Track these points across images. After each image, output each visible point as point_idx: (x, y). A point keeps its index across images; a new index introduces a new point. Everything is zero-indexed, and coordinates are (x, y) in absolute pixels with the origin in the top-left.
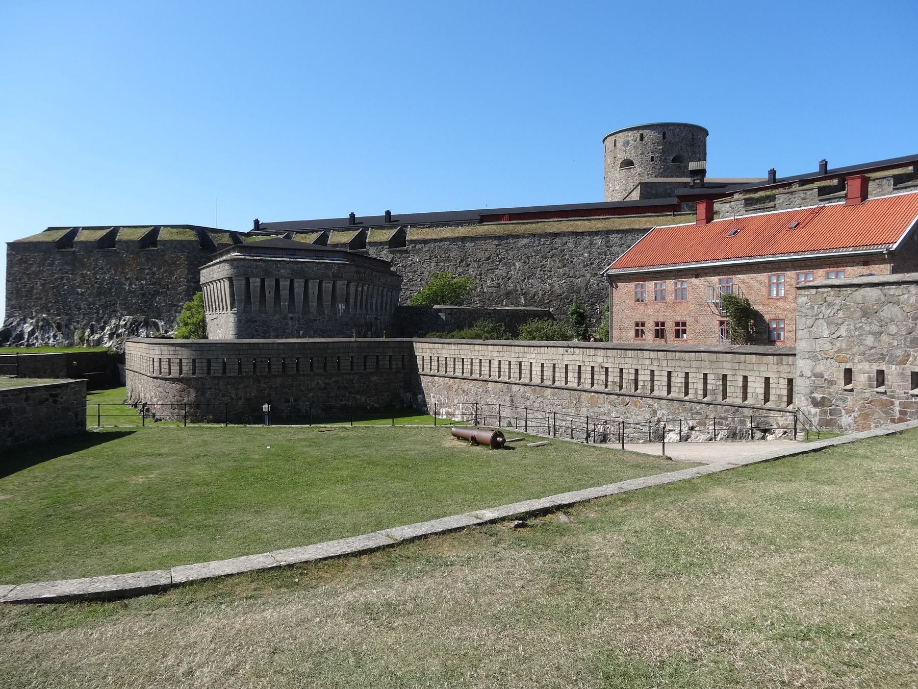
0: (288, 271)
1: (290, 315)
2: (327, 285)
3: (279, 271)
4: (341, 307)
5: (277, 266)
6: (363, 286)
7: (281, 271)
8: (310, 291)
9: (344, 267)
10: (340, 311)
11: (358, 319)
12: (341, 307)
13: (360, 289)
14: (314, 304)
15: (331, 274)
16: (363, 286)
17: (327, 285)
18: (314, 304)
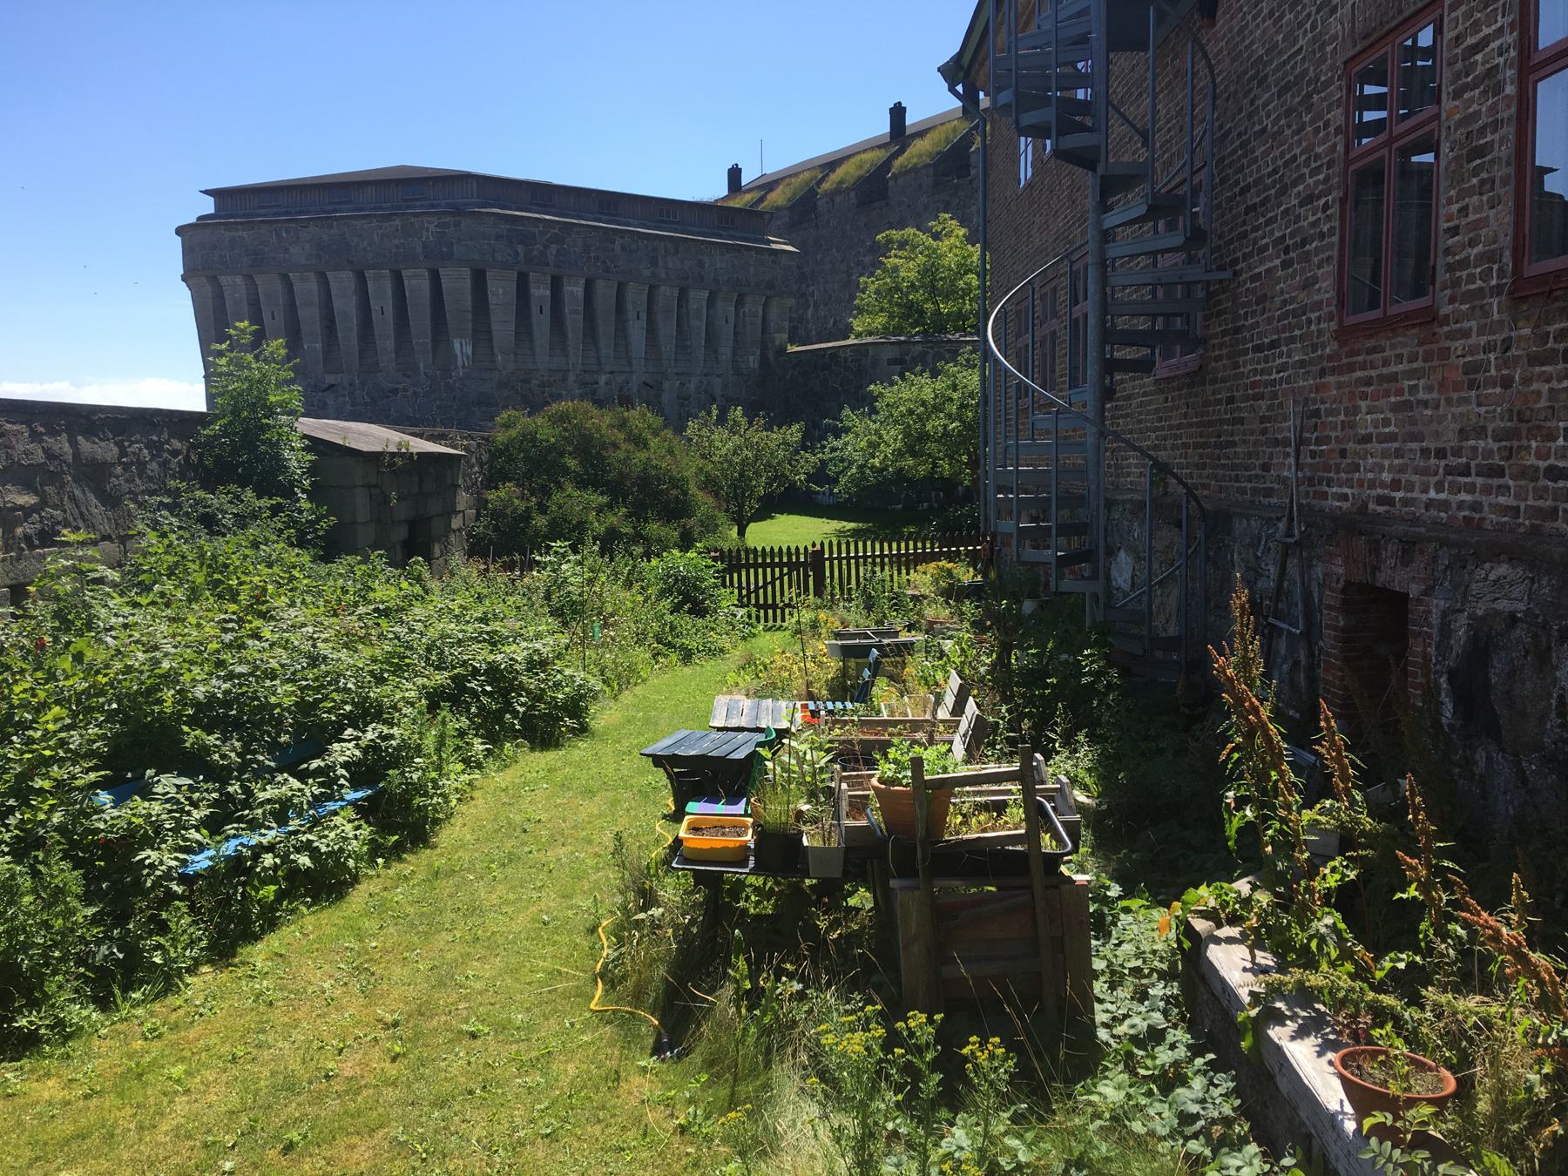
0: (307, 246)
1: (330, 379)
2: (417, 284)
3: (286, 251)
4: (462, 348)
5: (278, 235)
6: (556, 286)
7: (294, 250)
8: (375, 306)
9: (457, 224)
10: (460, 363)
11: (542, 385)
12: (462, 348)
13: (540, 292)
14: (386, 341)
15: (419, 250)
16: (556, 286)
17: (417, 284)
18: (386, 341)
